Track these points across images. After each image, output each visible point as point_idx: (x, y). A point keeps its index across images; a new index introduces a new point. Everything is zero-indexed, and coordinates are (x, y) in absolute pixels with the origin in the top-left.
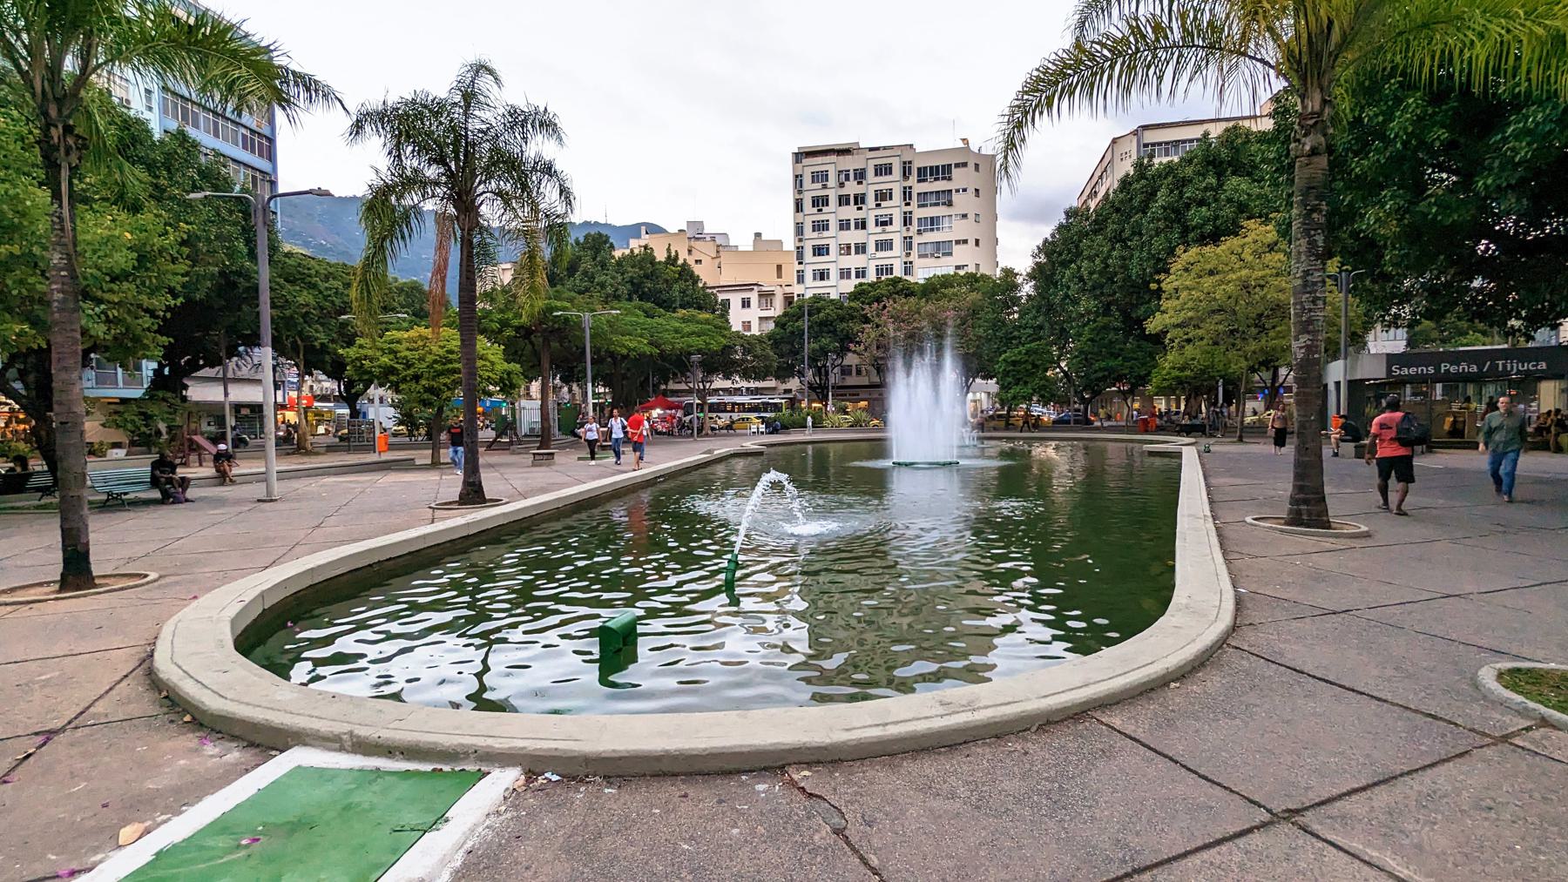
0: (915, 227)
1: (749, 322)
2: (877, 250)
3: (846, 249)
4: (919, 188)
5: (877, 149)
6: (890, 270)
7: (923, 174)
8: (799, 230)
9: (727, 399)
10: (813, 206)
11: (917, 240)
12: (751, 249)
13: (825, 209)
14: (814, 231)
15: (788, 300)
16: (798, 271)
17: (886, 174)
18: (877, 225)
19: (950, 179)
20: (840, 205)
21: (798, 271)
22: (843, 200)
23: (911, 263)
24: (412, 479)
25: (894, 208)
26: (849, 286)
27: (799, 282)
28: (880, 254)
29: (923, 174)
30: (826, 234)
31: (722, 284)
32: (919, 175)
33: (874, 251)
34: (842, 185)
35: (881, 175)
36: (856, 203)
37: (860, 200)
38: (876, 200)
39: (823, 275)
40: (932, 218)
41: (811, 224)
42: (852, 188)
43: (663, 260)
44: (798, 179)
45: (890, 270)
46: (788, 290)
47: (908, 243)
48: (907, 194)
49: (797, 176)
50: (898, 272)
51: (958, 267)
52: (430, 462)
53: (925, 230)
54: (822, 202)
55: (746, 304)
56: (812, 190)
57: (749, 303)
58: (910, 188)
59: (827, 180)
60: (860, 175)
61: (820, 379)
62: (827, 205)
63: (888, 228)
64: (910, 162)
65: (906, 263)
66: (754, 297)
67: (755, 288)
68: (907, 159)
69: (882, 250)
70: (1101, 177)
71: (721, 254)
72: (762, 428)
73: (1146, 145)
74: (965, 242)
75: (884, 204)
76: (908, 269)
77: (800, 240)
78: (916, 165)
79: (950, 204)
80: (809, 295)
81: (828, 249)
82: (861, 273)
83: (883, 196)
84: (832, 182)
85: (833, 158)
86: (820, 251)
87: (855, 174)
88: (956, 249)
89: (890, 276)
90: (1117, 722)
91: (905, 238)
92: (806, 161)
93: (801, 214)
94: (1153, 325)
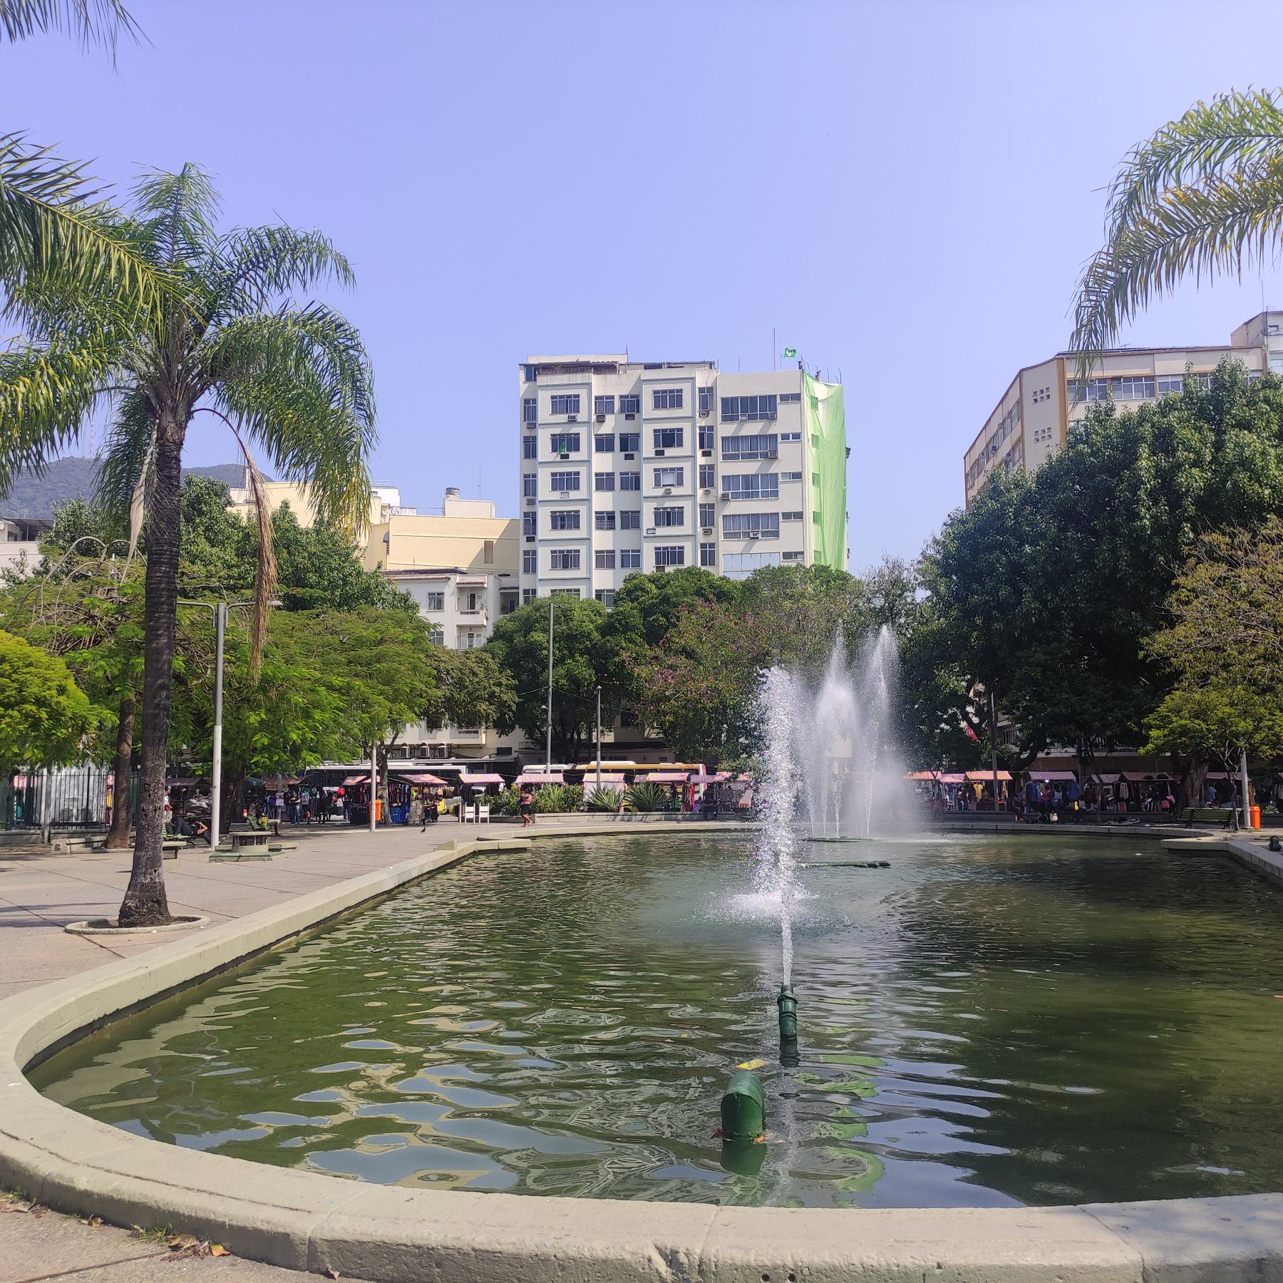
2: (657, 524)
4: (725, 430)
5: (657, 366)
6: (675, 555)
7: (737, 408)
10: (554, 450)
13: (573, 456)
14: (554, 488)
15: (508, 602)
16: (526, 553)
17: (672, 406)
19: (773, 418)
21: (526, 553)
23: (712, 545)
25: (688, 455)
26: (606, 580)
27: (526, 571)
30: (573, 495)
33: (652, 525)
34: (601, 419)
35: (664, 407)
36: (624, 448)
38: (656, 445)
39: (566, 560)
40: (746, 477)
44: (529, 409)
45: (675, 555)
46: (507, 582)
48: (706, 440)
50: (691, 558)
51: (787, 556)
53: (736, 496)
58: (711, 428)
62: (577, 449)
64: (710, 390)
65: (703, 546)
74: (799, 516)
75: (669, 452)
76: (708, 555)
78: (721, 393)
79: (772, 456)
82: (631, 558)
83: (668, 439)
86: (564, 520)
88: (785, 527)
89: (680, 567)
92: (542, 380)
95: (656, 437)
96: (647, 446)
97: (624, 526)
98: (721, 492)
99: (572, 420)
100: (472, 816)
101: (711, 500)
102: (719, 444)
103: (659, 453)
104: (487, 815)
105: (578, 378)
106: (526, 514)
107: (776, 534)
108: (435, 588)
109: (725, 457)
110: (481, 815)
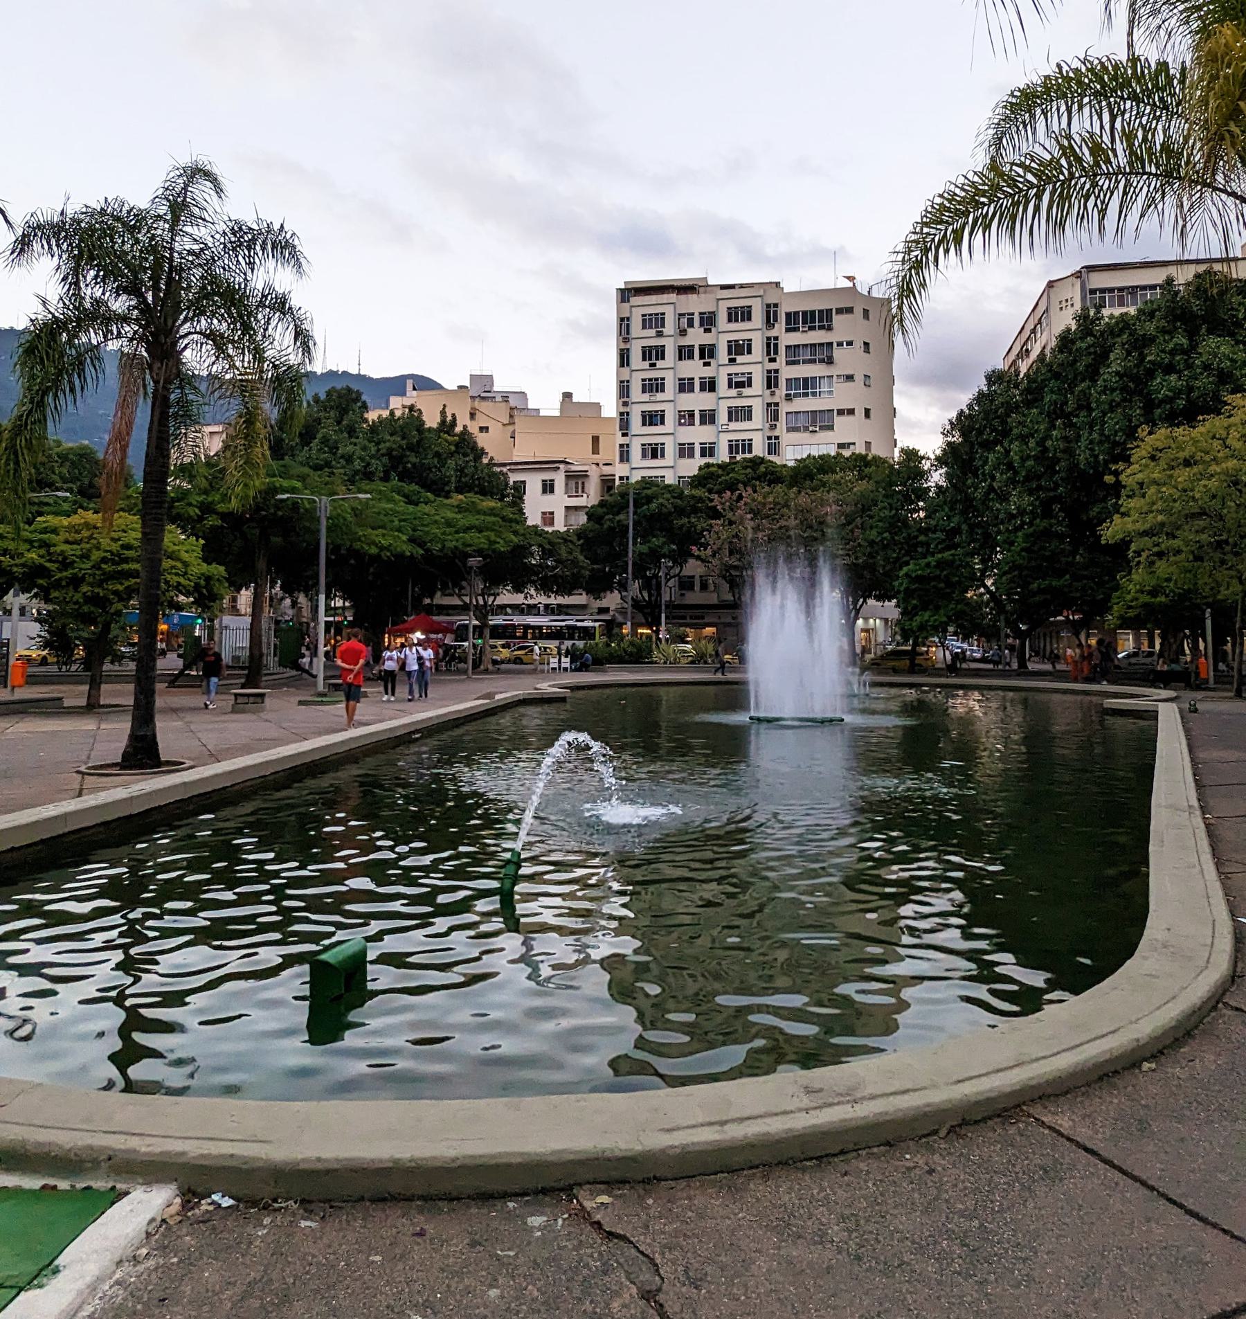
0: (782, 390)
1: (552, 513)
2: (730, 420)
3: (687, 418)
6: (748, 446)
8: (624, 390)
9: (518, 620)
10: (644, 359)
11: (785, 408)
12: (557, 413)
13: (660, 364)
14: (644, 391)
15: (607, 483)
16: (621, 446)
17: (743, 320)
18: (730, 386)
19: (830, 328)
20: (680, 359)
21: (621, 446)
22: (685, 353)
23: (777, 438)
24: (55, 728)
26: (691, 467)
27: (622, 460)
28: (734, 426)
29: (793, 322)
30: (660, 396)
31: (516, 459)
32: (788, 322)
34: (683, 333)
35: (737, 321)
36: (702, 357)
37: (707, 353)
38: (730, 353)
39: (655, 452)
40: (806, 380)
41: (640, 383)
42: (697, 337)
43: (435, 426)
44: (624, 324)
45: (748, 446)
46: (607, 470)
47: (772, 412)
48: (771, 347)
49: (622, 319)
50: (759, 450)
51: (841, 446)
52: (84, 704)
53: (796, 395)
54: (653, 354)
55: (548, 487)
56: (643, 338)
57: (552, 486)
58: (776, 338)
59: (663, 326)
60: (708, 321)
61: (650, 595)
62: (663, 358)
63: (746, 391)
64: (776, 305)
65: (769, 438)
66: (559, 479)
67: (562, 466)
68: (772, 301)
69: (737, 420)
70: (1034, 331)
71: (516, 420)
72: (566, 662)
73: (1093, 292)
74: (851, 412)
75: (739, 359)
76: (773, 447)
77: (625, 404)
79: (830, 361)
80: (636, 477)
81: (663, 417)
82: (708, 450)
83: (738, 349)
84: (670, 328)
85: (673, 297)
86: (653, 418)
87: (702, 319)
88: (838, 420)
89: (748, 456)
90: (1064, 1123)
91: (769, 405)
92: (635, 300)
93: (626, 370)
94: (1111, 531)
95: (730, 347)
96: (722, 354)
97: (703, 422)
98: (785, 392)
99: (660, 334)
100: (556, 665)
101: (776, 400)
102: (782, 350)
103: (732, 361)
104: (568, 665)
105: (665, 298)
106: (622, 414)
107: (831, 428)
108: (548, 476)
109: (788, 363)
110: (563, 665)
